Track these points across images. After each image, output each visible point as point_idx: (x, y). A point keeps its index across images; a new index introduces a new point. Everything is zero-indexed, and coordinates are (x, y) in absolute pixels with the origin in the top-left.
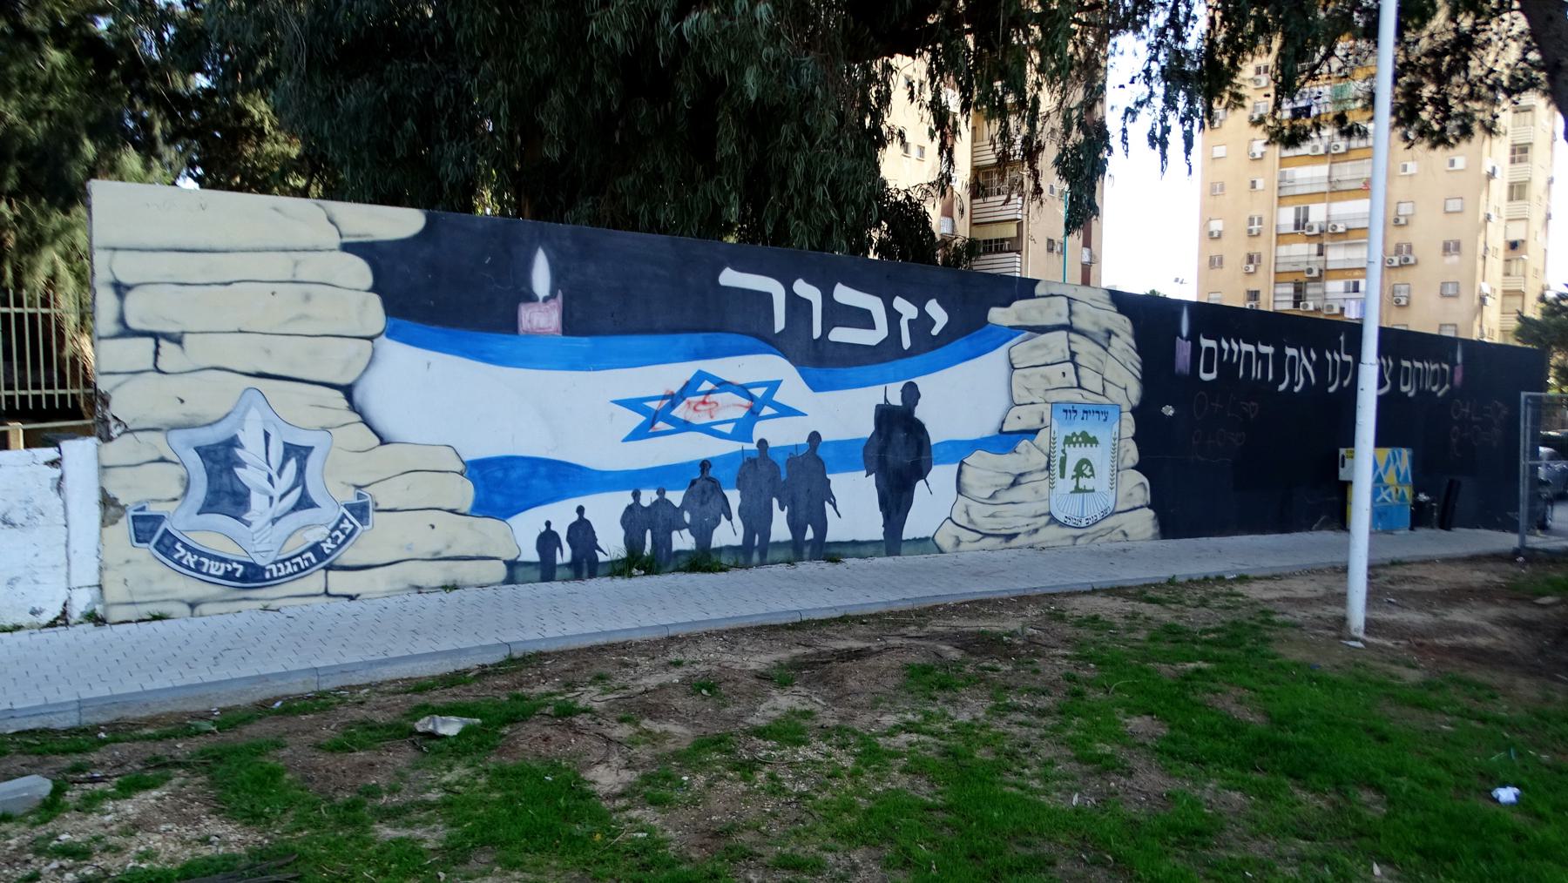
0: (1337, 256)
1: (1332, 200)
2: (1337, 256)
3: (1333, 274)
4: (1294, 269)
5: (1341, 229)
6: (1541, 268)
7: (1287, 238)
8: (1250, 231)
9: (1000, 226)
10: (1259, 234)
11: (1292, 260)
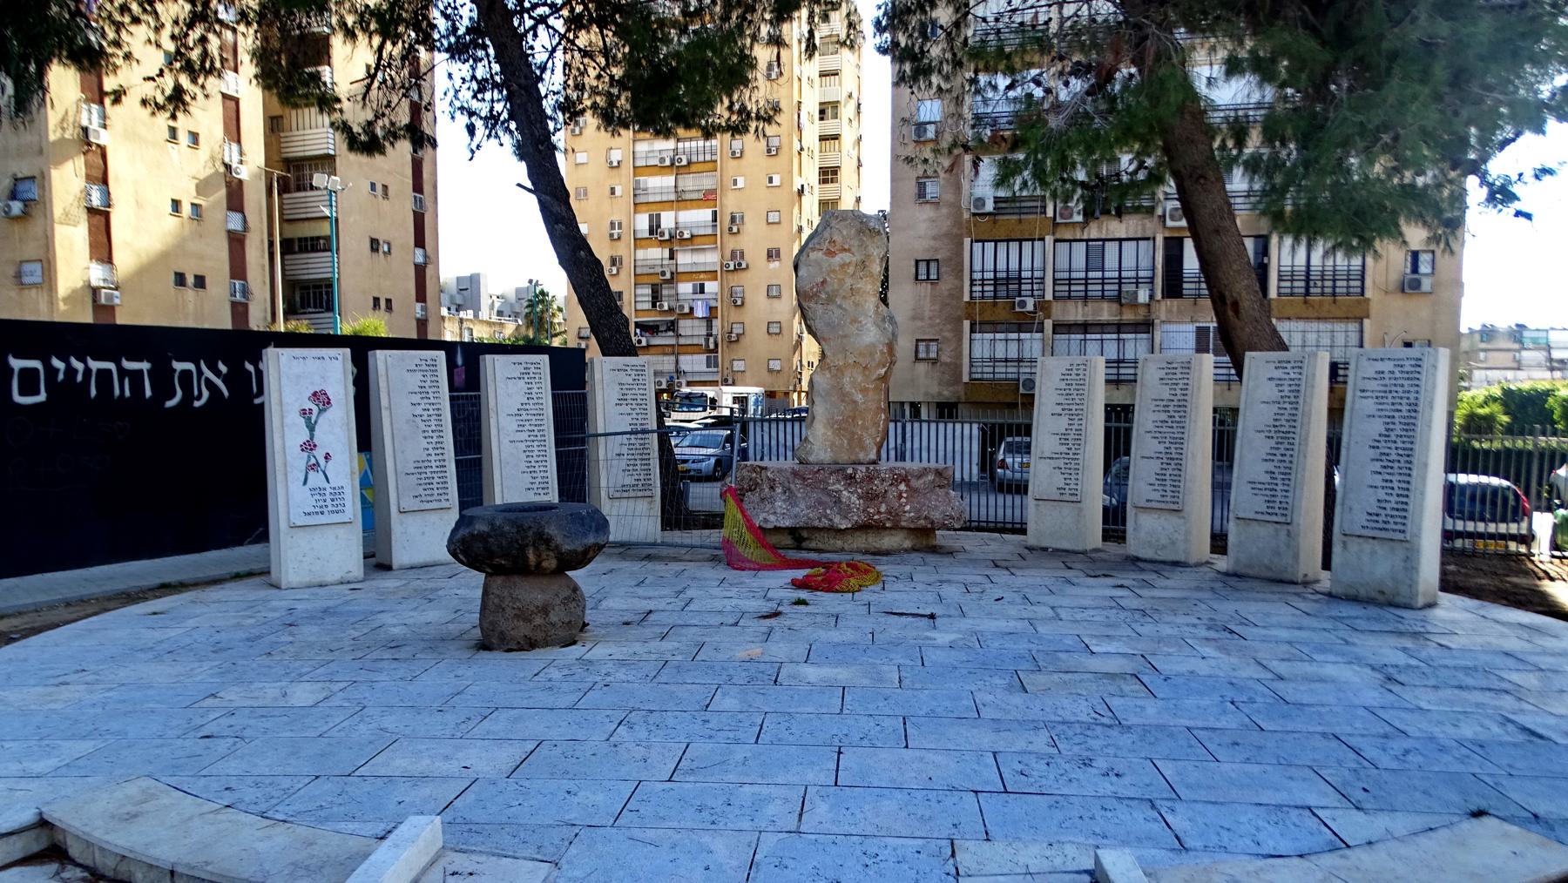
0: (685, 259)
1: (678, 209)
2: (685, 259)
3: (683, 277)
4: (652, 271)
5: (686, 236)
7: (643, 243)
8: (611, 235)
9: (312, 224)
10: (619, 238)
11: (649, 263)
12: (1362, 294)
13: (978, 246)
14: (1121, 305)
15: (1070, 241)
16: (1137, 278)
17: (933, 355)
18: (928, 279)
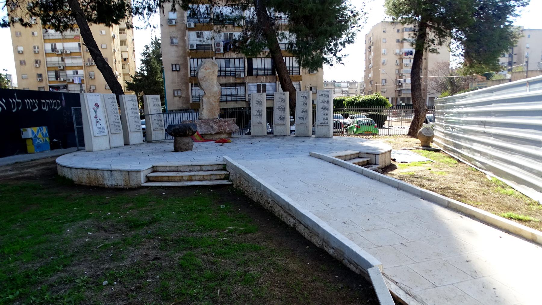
0: (69, 62)
1: (64, 42)
2: (69, 62)
4: (54, 66)
7: (50, 55)
8: (35, 52)
10: (38, 53)
11: (53, 63)
12: (300, 74)
13: (192, 60)
14: (236, 78)
15: (220, 58)
16: (240, 70)
17: (179, 95)
18: (176, 70)
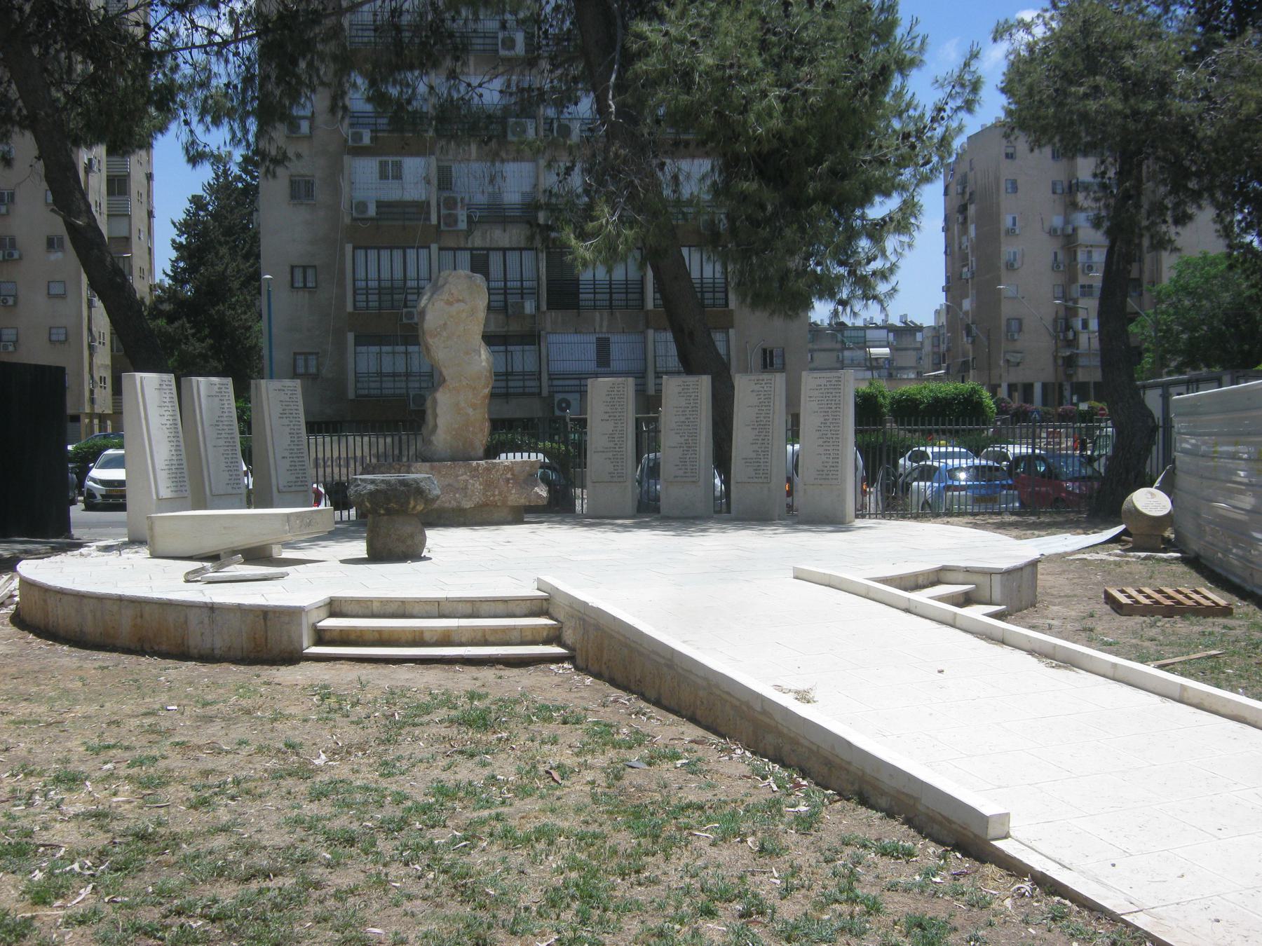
6: (146, 267)
12: (727, 305)
13: (361, 254)
14: (507, 316)
15: (455, 249)
16: (522, 288)
17: (313, 370)
18: (305, 286)
